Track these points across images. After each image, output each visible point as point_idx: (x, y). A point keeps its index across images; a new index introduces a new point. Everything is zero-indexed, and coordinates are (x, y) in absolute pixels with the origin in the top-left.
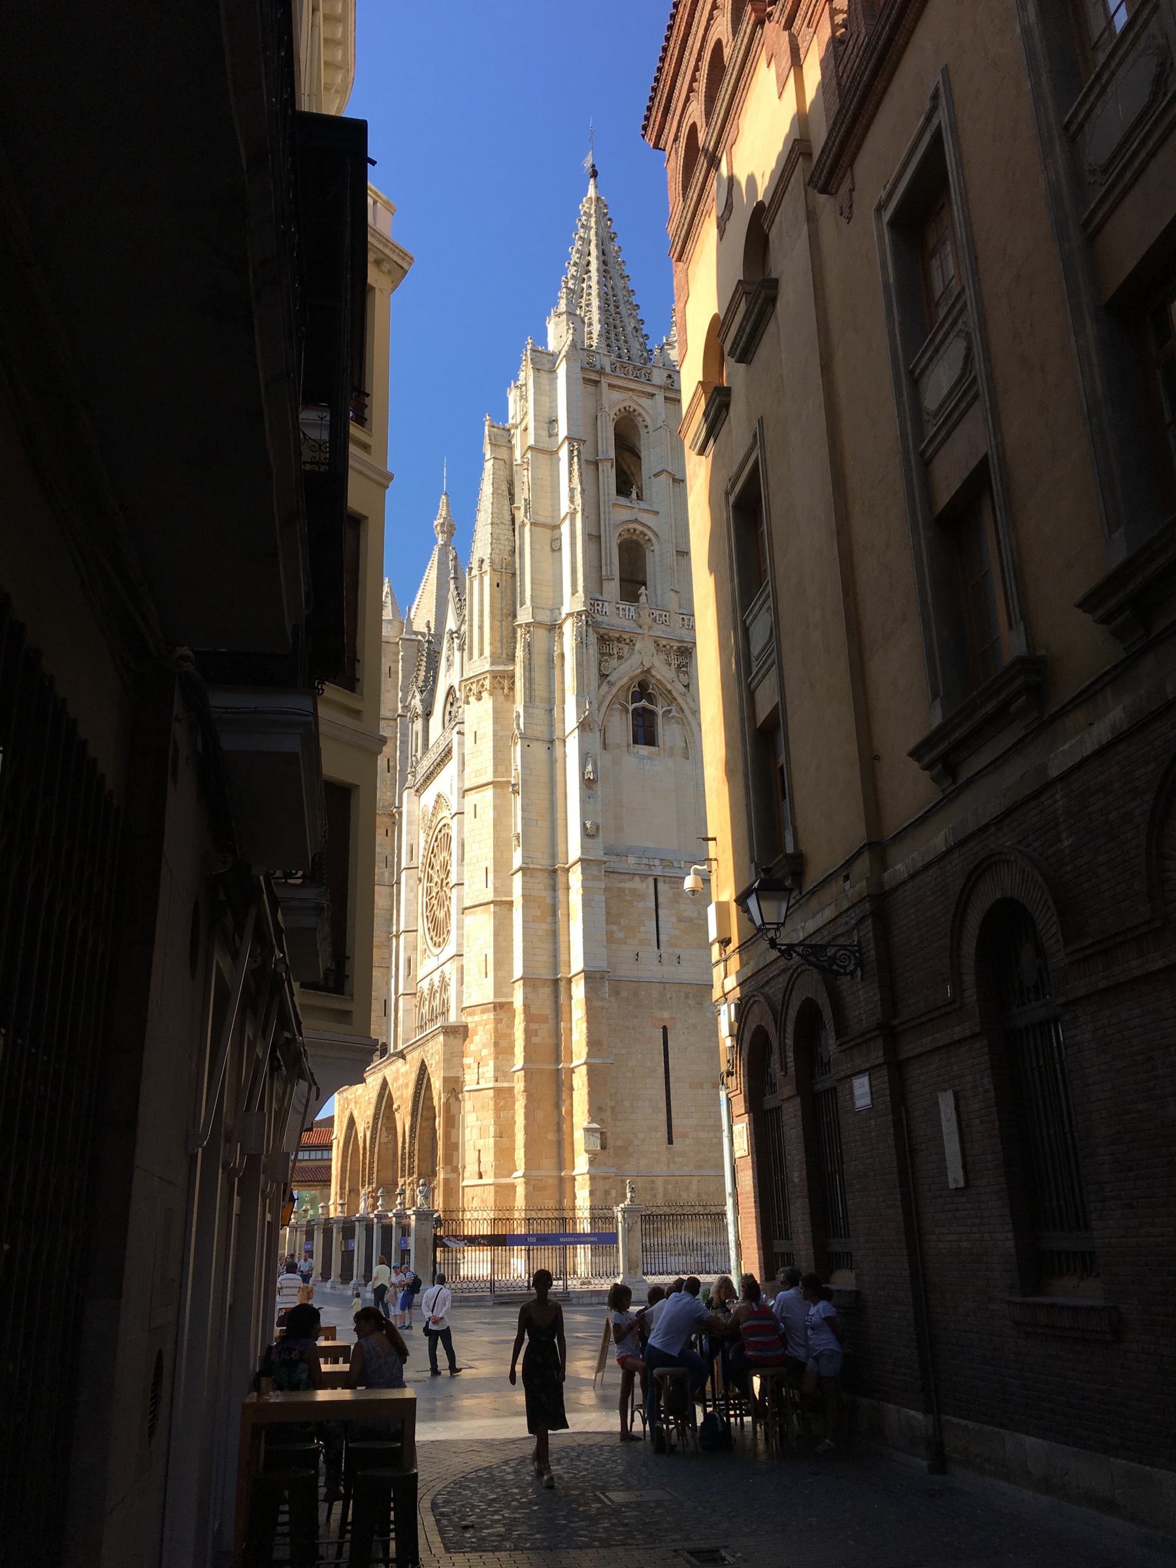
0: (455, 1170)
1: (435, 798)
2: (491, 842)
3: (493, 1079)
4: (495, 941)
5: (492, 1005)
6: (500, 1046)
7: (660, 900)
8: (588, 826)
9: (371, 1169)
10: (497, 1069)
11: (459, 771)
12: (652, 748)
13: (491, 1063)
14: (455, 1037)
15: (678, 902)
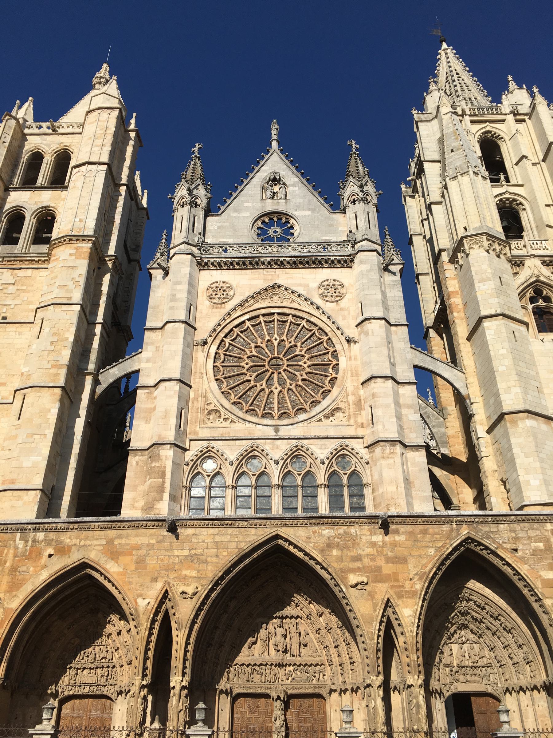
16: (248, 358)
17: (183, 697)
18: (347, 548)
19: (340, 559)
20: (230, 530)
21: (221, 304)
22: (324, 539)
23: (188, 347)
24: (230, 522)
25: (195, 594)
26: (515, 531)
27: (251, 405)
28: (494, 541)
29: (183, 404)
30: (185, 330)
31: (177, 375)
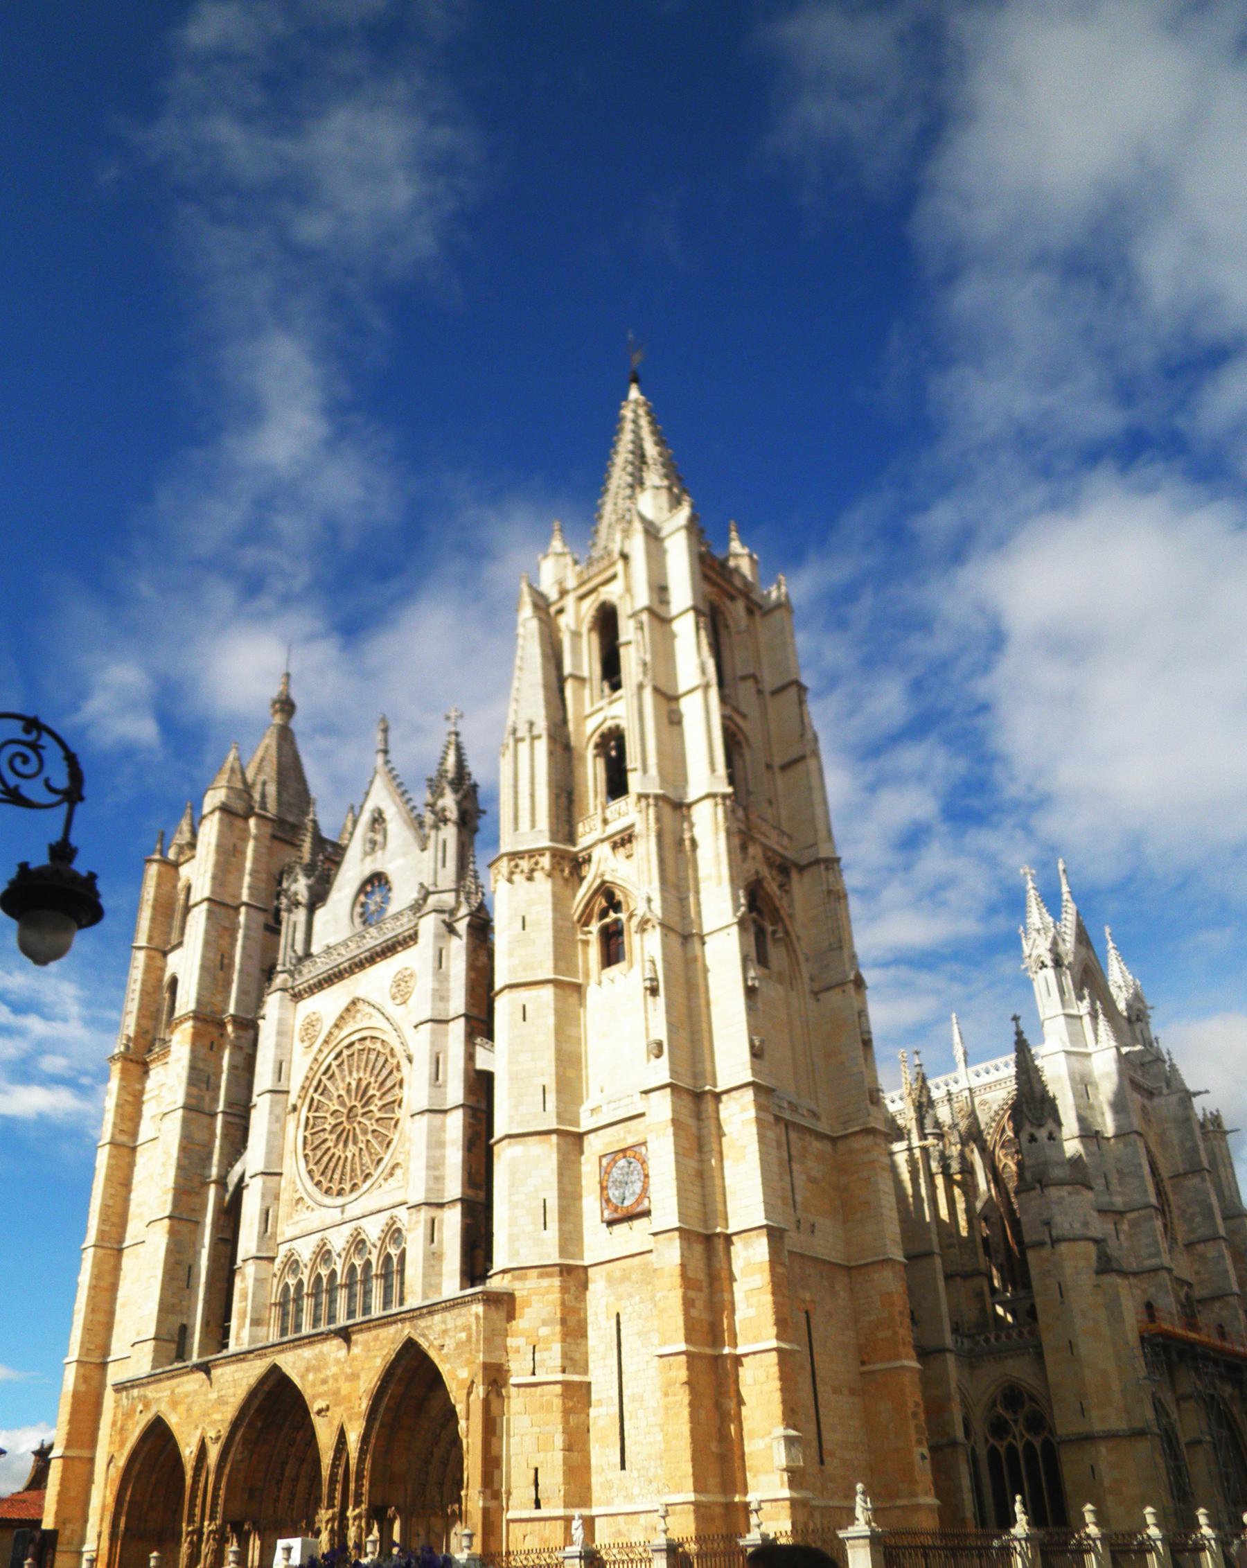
0: (496, 1495)
1: (345, 1002)
2: (550, 1054)
3: (560, 1369)
4: (560, 1182)
5: (558, 1268)
6: (569, 1324)
7: (794, 1152)
8: (757, 1043)
9: (215, 1496)
10: (565, 1355)
11: (434, 968)
12: (766, 972)
13: (557, 1348)
14: (497, 1308)
15: (805, 1157)
16: (332, 1114)
17: (211, 1541)
18: (317, 1369)
19: (313, 1385)
20: (245, 1365)
21: (309, 1047)
22: (302, 1365)
23: (277, 1122)
24: (241, 1356)
25: (218, 1438)
26: (444, 1322)
27: (330, 1181)
28: (428, 1340)
29: (269, 1201)
30: (272, 1101)
31: (261, 1168)
